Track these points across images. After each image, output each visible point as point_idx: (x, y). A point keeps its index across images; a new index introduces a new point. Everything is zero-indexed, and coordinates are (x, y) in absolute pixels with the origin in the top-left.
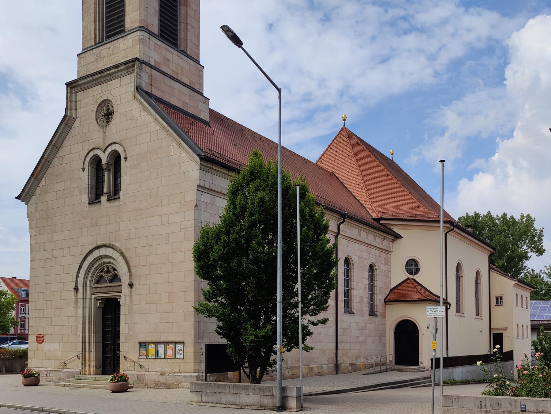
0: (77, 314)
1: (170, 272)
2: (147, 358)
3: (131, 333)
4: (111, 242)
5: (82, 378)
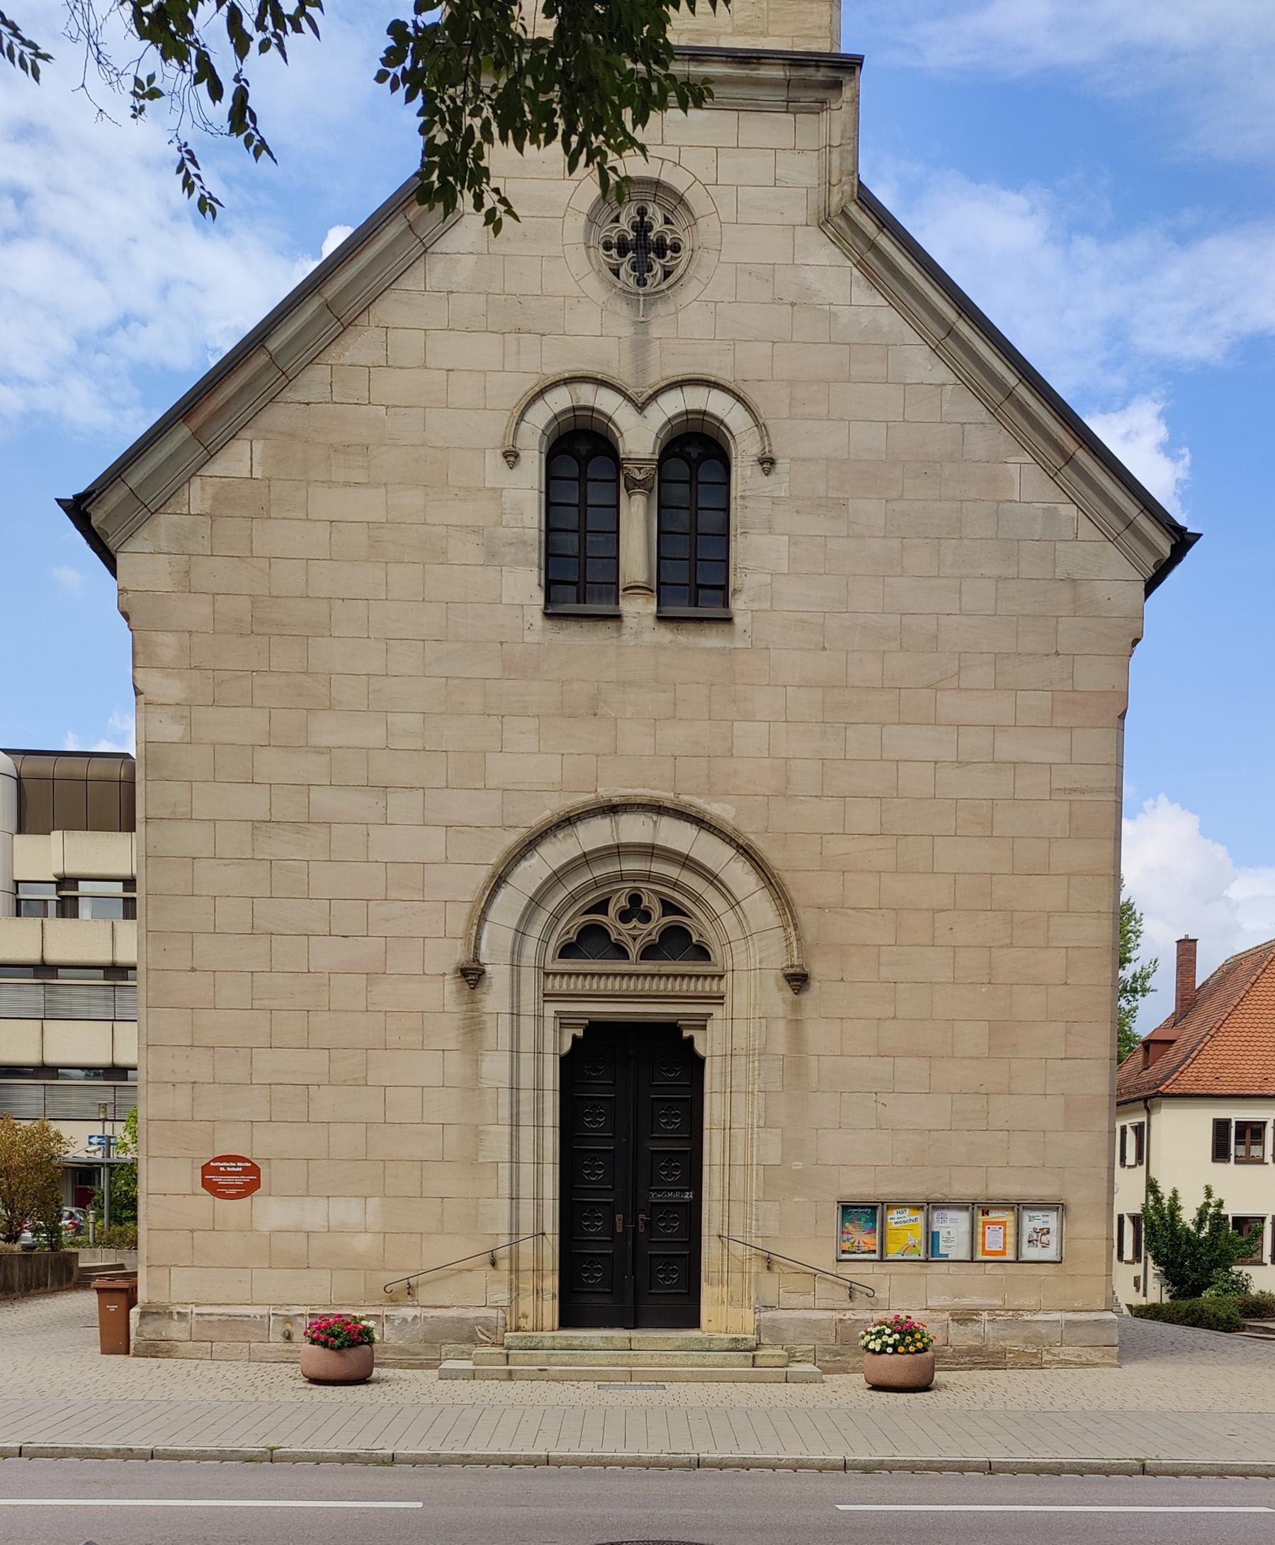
0: (477, 1077)
1: (1002, 947)
2: (881, 1260)
3: (797, 1165)
4: (681, 797)
5: (548, 1343)
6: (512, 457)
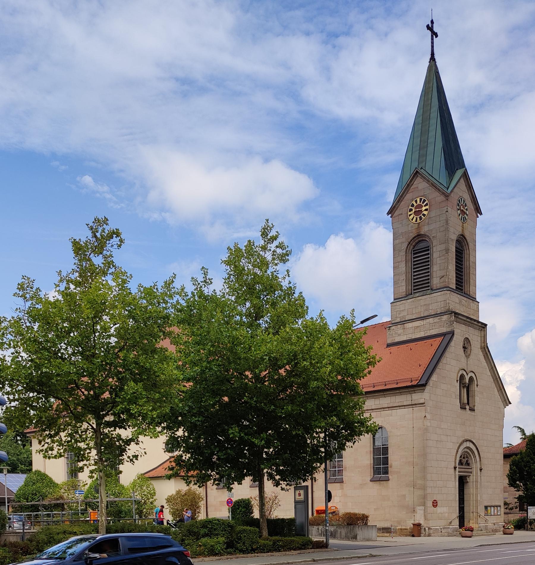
6: (457, 381)
